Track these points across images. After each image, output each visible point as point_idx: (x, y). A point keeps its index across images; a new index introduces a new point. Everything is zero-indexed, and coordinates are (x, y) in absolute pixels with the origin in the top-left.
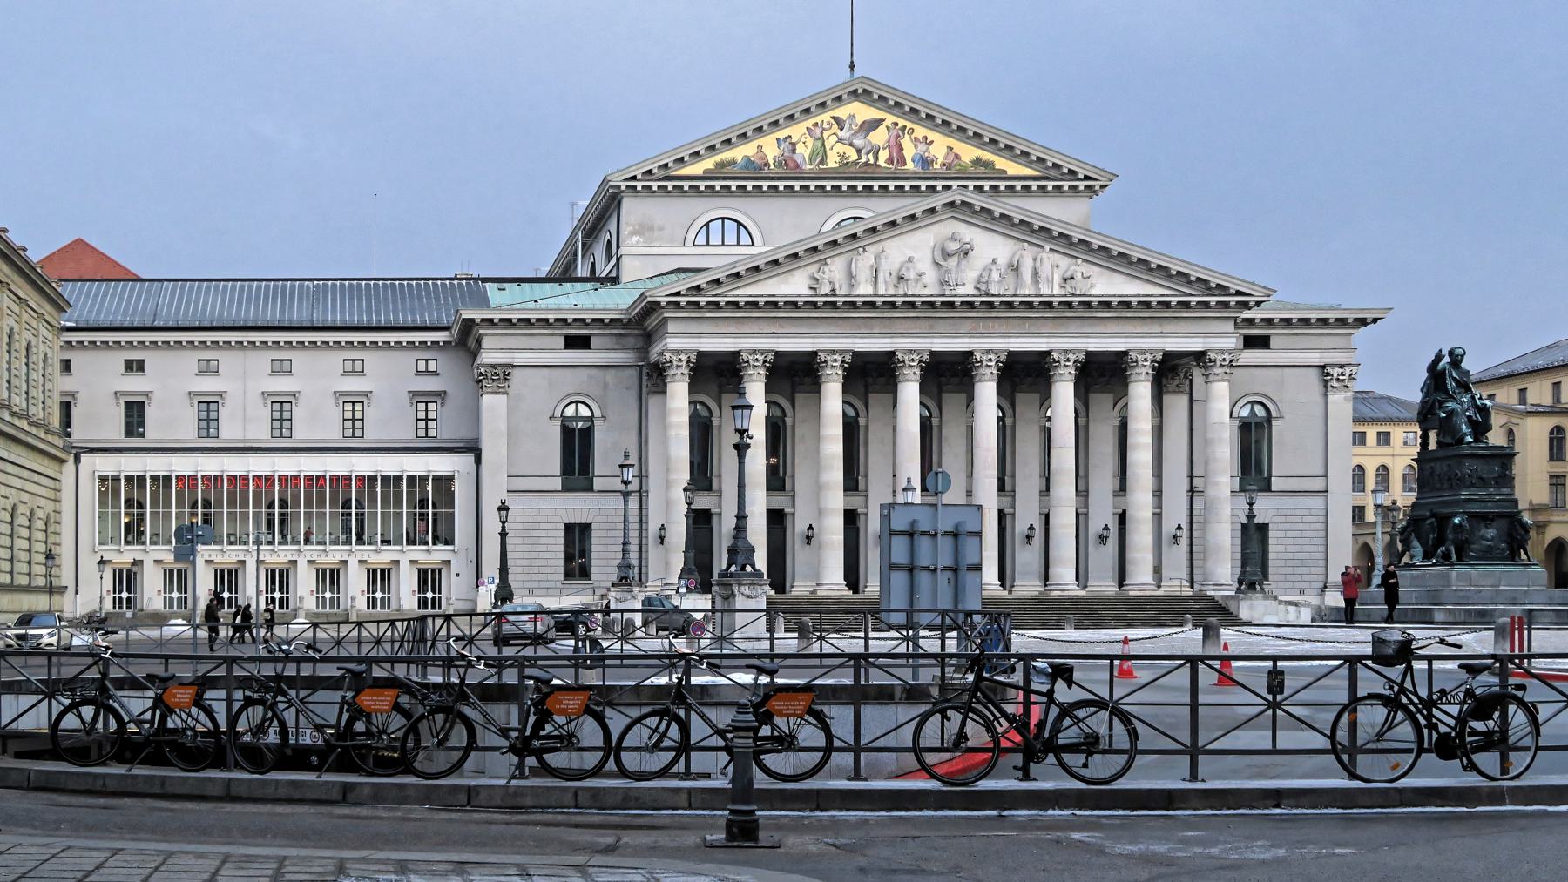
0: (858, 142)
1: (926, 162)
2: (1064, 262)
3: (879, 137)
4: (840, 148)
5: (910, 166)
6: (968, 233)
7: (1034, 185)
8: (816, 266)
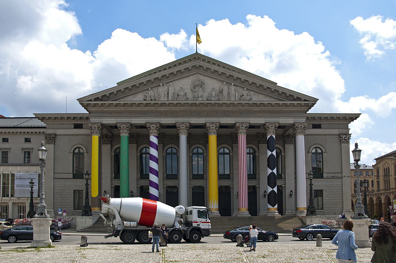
2: (240, 90)
6: (202, 77)
8: (146, 92)
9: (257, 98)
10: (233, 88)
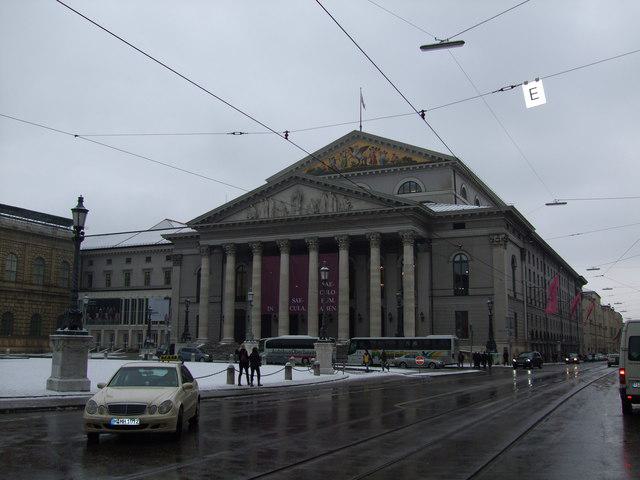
0: (359, 156)
1: (384, 161)
3: (367, 153)
4: (352, 160)
5: (379, 164)
7: (424, 166)
9: (359, 206)
10: (331, 197)
